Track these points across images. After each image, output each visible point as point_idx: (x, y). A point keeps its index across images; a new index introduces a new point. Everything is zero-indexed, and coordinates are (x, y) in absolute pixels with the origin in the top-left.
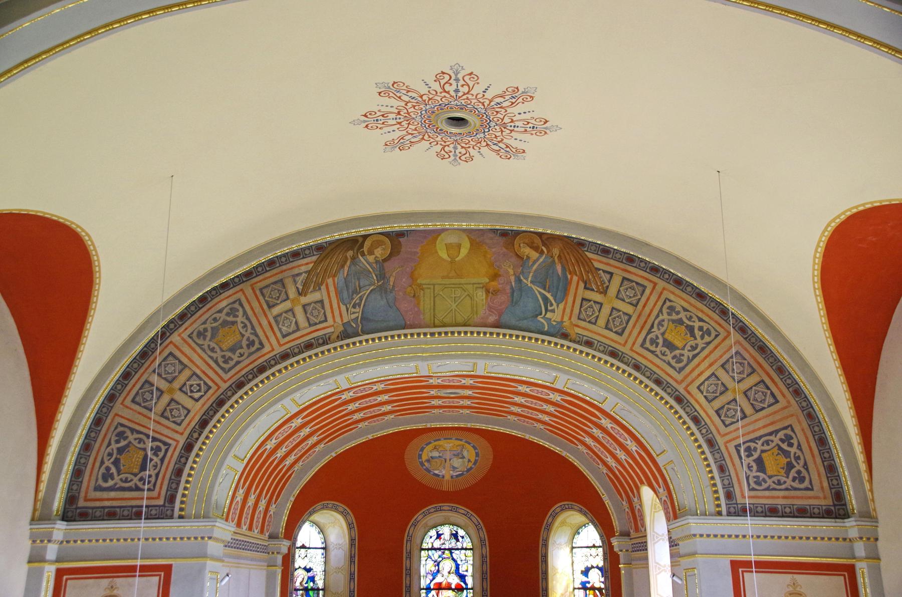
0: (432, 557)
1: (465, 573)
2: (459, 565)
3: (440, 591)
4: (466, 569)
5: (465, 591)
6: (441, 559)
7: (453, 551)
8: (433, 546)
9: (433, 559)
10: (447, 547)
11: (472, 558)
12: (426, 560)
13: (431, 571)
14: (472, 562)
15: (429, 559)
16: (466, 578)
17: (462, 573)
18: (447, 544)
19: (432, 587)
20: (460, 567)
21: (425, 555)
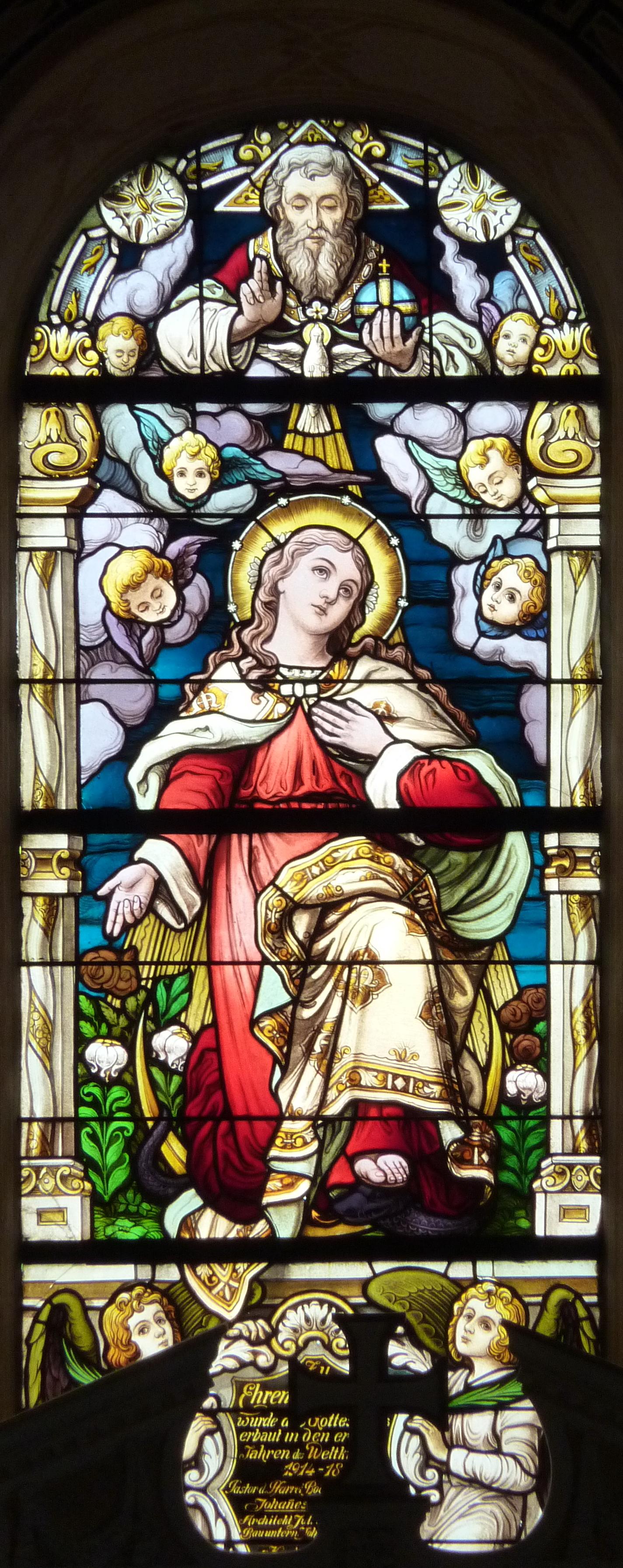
0: (144, 468)
2: (453, 560)
3: (239, 845)
7: (381, 411)
9: (158, 491)
13: (131, 623)
15: (109, 500)
18: (316, 334)
19: (146, 802)
20: (463, 576)
21: (64, 455)
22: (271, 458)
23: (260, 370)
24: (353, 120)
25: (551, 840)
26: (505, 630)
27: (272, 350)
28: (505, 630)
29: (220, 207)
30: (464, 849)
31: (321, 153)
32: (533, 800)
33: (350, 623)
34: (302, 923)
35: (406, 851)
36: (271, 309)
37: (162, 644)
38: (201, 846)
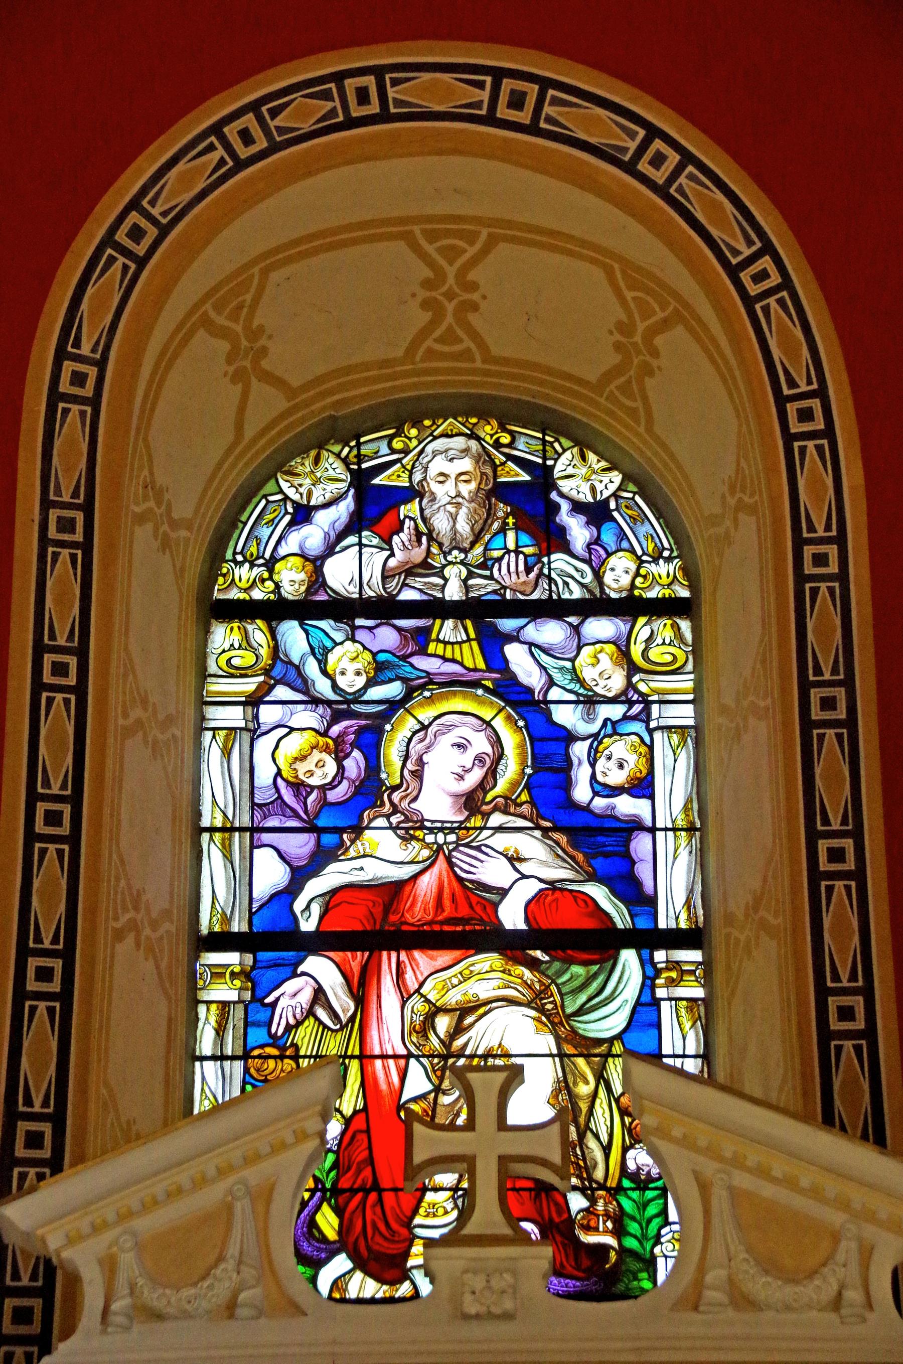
0: (312, 669)
1: (626, 806)
2: (569, 737)
3: (388, 961)
4: (634, 763)
5: (629, 957)
6: (393, 690)
7: (508, 624)
8: (317, 580)
9: (323, 687)
10: (453, 592)
11: (685, 683)
12: (254, 701)
14: (684, 715)
15: (282, 692)
16: (641, 844)
17: (600, 803)
19: (308, 925)
20: (579, 750)
21: (245, 659)
22: (416, 661)
23: (408, 595)
24: (484, 416)
25: (660, 956)
26: (615, 791)
27: (418, 582)
28: (615, 791)
29: (376, 481)
30: (585, 963)
31: (459, 442)
32: (643, 923)
33: (483, 786)
34: (443, 1023)
35: (533, 965)
36: (418, 554)
37: (324, 804)
38: (356, 960)
